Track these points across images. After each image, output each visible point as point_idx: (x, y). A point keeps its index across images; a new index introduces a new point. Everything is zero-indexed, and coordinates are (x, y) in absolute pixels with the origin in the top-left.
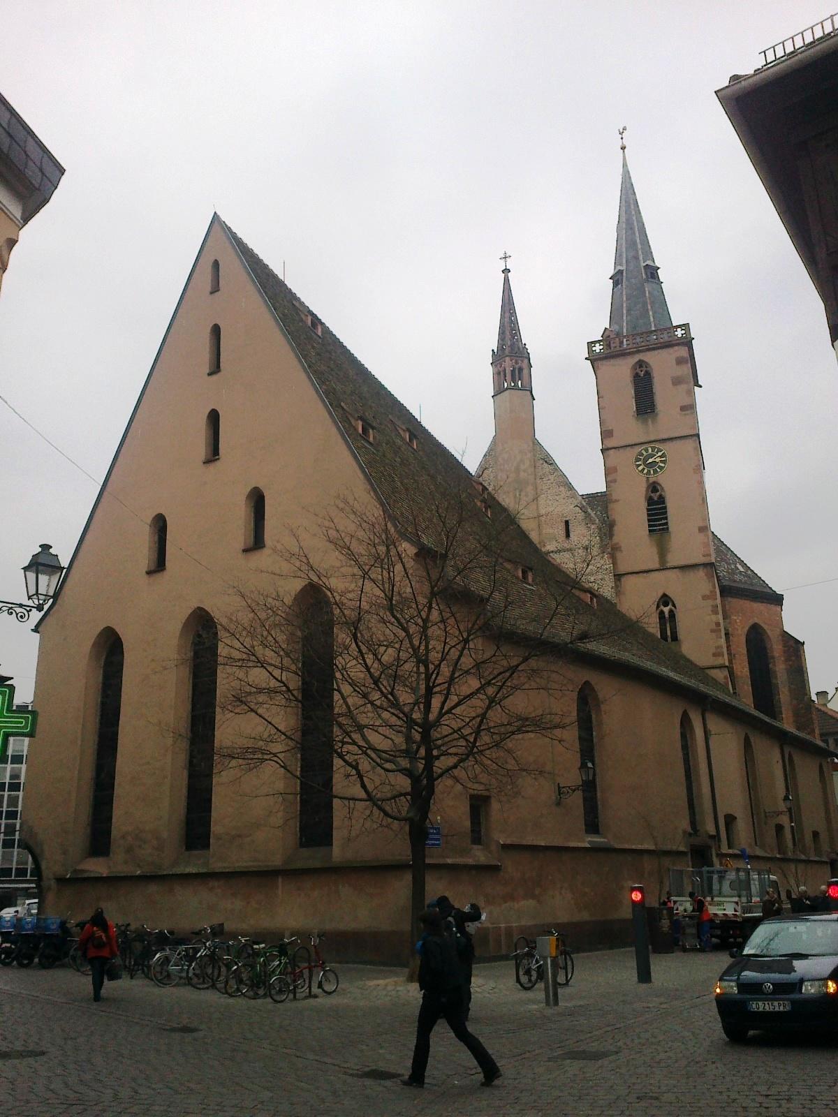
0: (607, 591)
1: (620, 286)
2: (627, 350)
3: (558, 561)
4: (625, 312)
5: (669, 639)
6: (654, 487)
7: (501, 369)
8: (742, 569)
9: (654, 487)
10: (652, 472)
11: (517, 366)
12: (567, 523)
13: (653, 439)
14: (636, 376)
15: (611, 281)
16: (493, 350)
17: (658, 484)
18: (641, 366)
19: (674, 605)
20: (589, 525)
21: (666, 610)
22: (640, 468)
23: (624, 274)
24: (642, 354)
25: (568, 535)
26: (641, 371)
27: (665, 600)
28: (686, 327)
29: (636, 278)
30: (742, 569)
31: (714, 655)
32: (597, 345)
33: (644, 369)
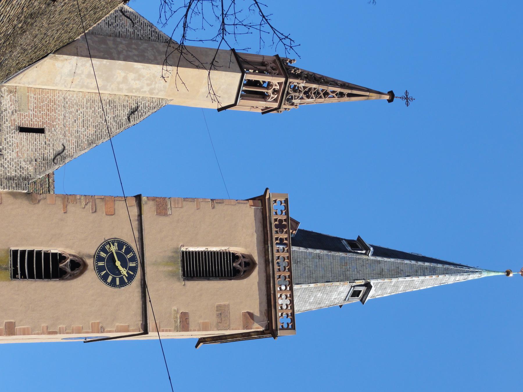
1: (349, 248)
6: (78, 266)
7: (269, 68)
10: (101, 264)
12: (41, 131)
13: (148, 269)
15: (355, 239)
17: (82, 273)
18: (247, 264)
20: (34, 163)
24: (263, 266)
25: (23, 130)
26: (240, 264)
33: (242, 269)
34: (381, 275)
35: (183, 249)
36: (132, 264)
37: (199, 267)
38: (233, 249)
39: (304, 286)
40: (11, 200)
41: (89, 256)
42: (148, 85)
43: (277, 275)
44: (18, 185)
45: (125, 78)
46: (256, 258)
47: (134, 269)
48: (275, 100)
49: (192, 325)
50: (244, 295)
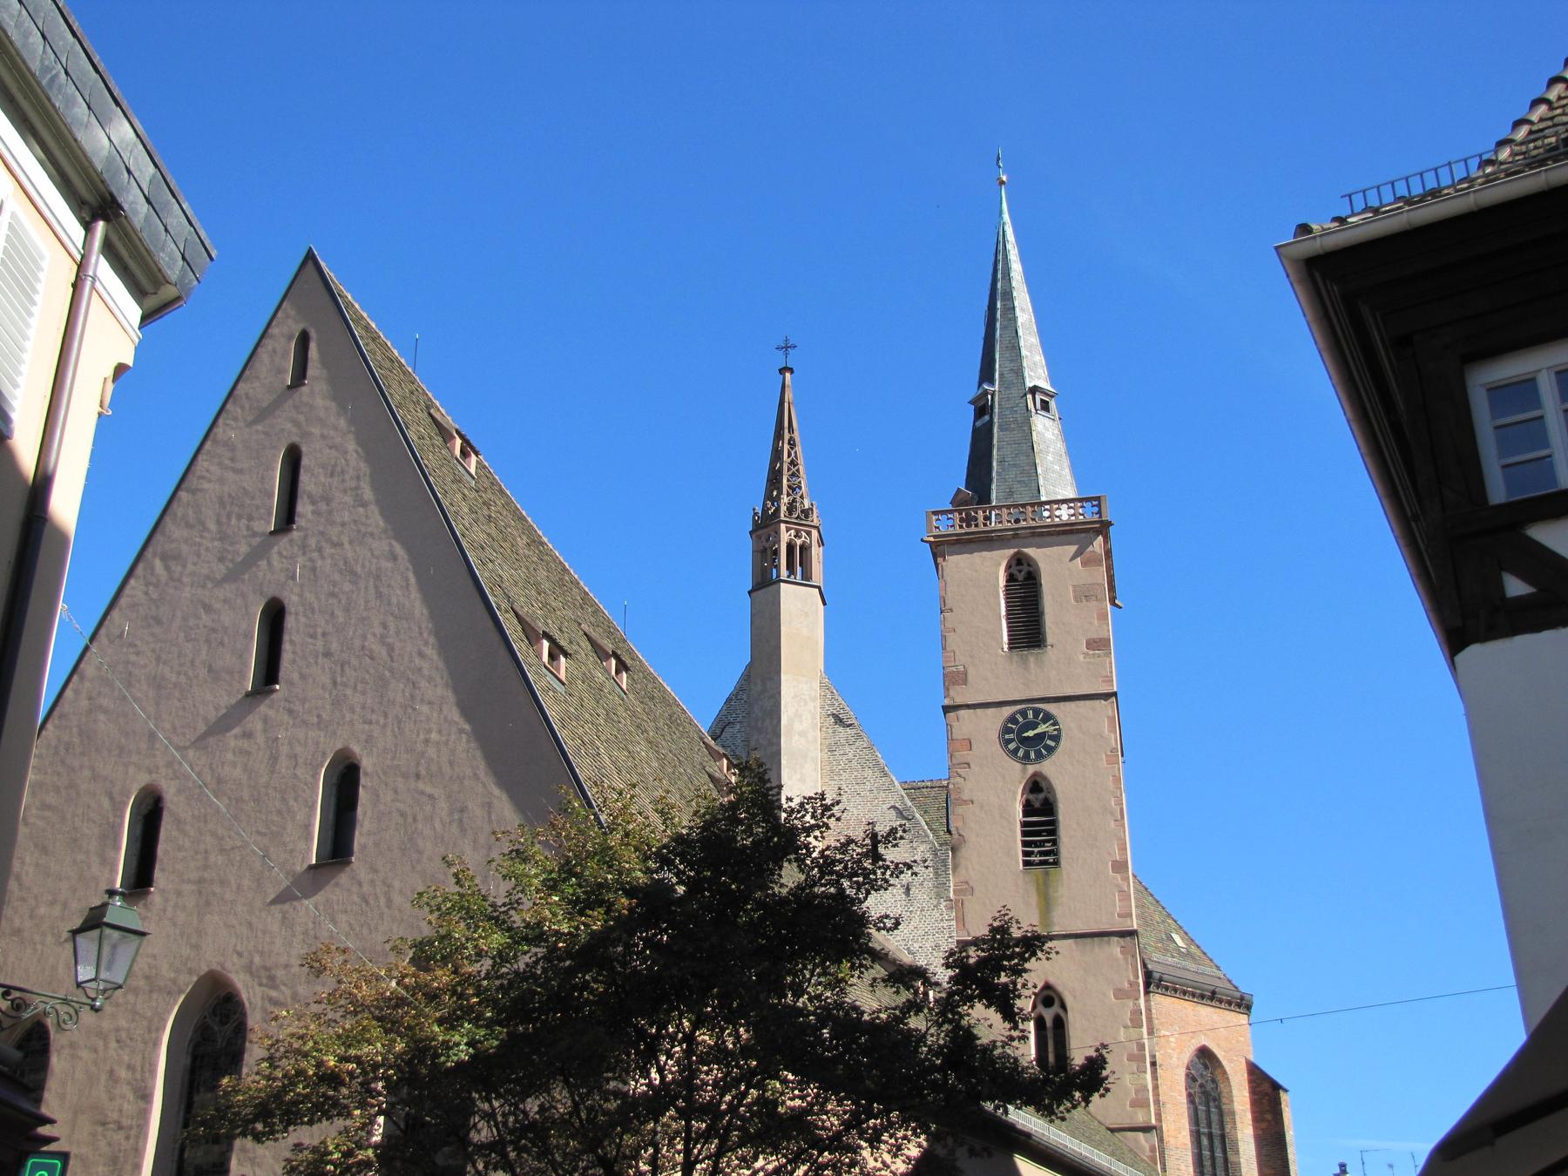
1: (987, 418)
6: (1036, 786)
8: (1180, 943)
9: (1036, 786)
10: (1033, 755)
11: (799, 542)
13: (1036, 695)
17: (1045, 778)
19: (1063, 1006)
21: (1048, 1015)
22: (1012, 746)
30: (1180, 943)
31: (1134, 1104)
33: (1025, 568)
34: (1019, 372)
35: (1006, 647)
36: (1030, 715)
37: (1028, 629)
38: (1002, 582)
39: (1041, 482)
40: (962, 870)
41: (1024, 771)
43: (1033, 524)
44: (944, 862)
45: (802, 734)
46: (1012, 551)
47: (1036, 712)
48: (809, 533)
49: (1103, 635)
50: (1056, 567)
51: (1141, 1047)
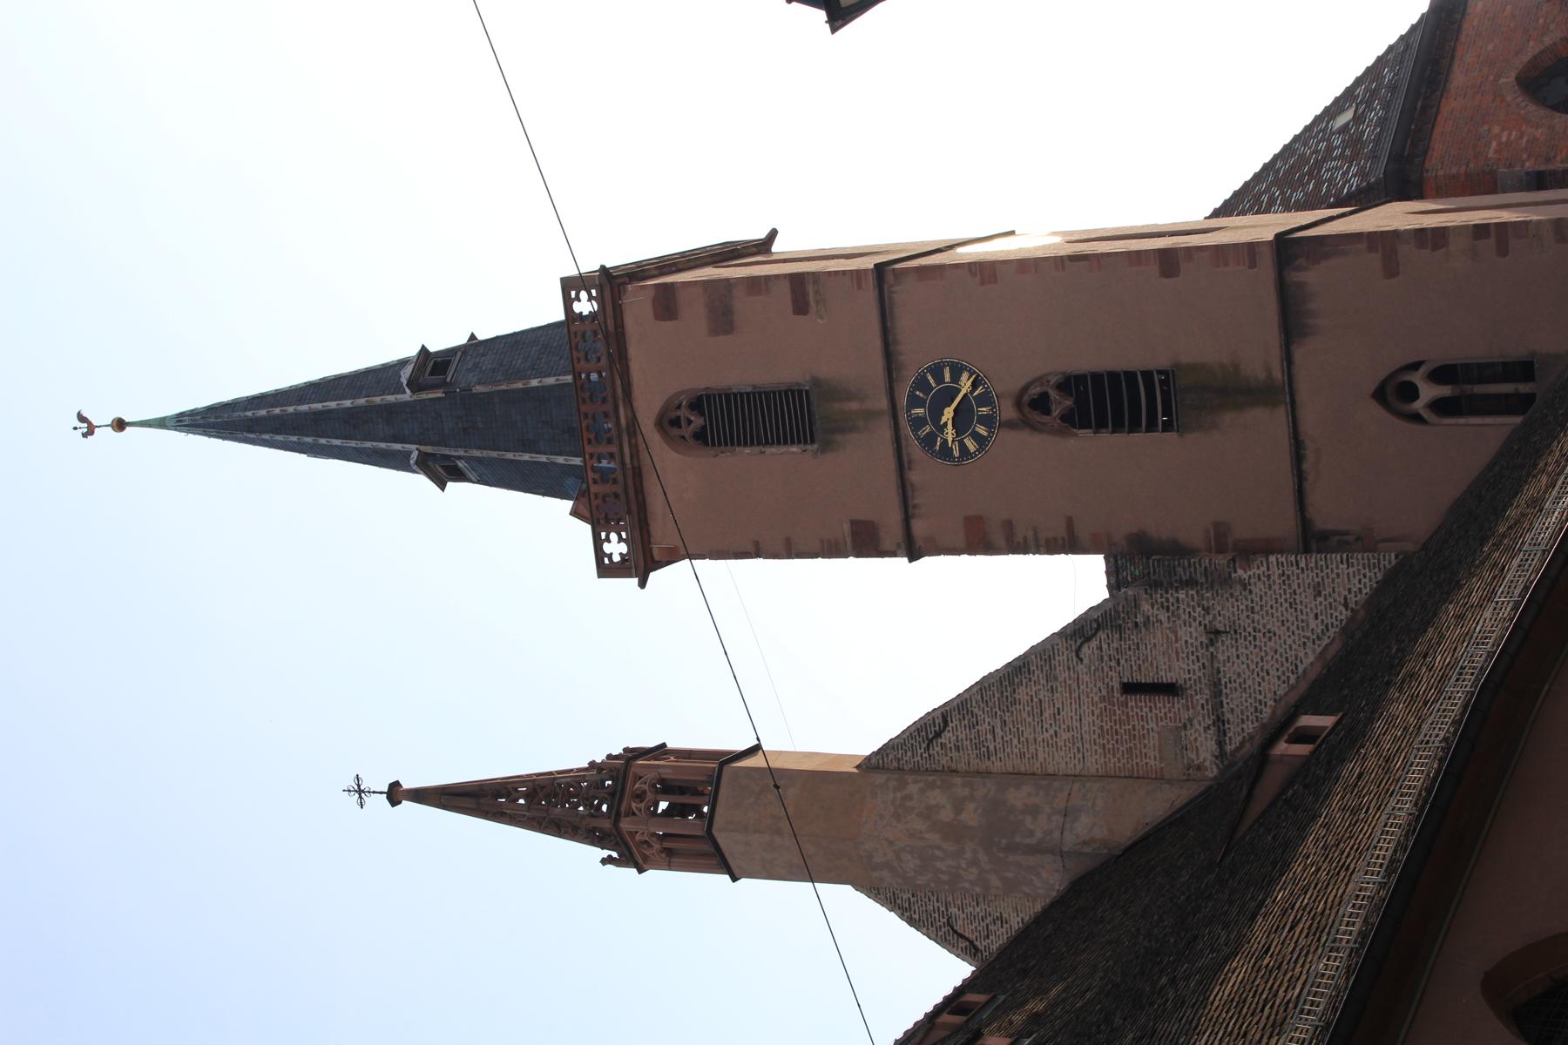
0: (1351, 580)
1: (461, 464)
2: (623, 463)
3: (1250, 727)
4: (526, 457)
5: (1524, 388)
7: (657, 846)
8: (1346, 117)
9: (1033, 406)
12: (1130, 688)
14: (701, 437)
15: (450, 485)
16: (604, 861)
17: (1025, 389)
18: (676, 423)
19: (1415, 366)
20: (1140, 619)
21: (1428, 392)
23: (429, 449)
25: (1170, 689)
26: (690, 422)
27: (1394, 393)
28: (570, 286)
29: (433, 415)
30: (1346, 117)
32: (607, 548)
33: (684, 413)
42: (909, 797)
45: (958, 808)
51: (1481, 230)
